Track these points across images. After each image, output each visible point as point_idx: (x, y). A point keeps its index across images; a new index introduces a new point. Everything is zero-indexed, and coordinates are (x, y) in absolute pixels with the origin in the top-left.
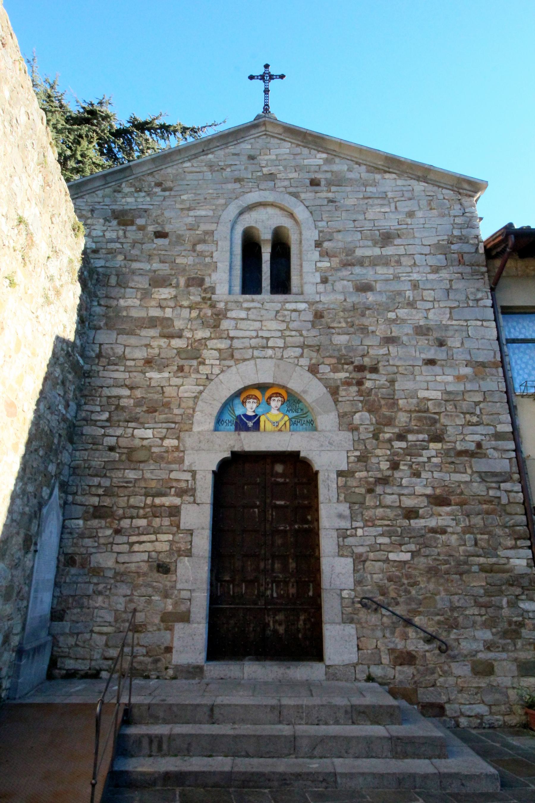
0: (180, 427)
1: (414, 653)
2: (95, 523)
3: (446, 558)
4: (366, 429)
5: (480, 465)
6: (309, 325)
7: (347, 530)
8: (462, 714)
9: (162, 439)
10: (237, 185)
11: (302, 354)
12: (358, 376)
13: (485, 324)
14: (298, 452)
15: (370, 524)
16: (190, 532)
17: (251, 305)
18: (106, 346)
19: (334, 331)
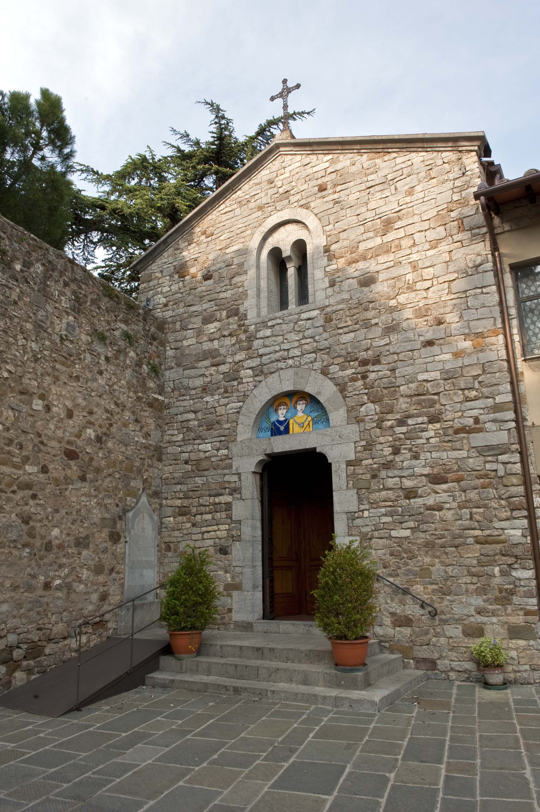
0: (228, 439)
1: (411, 617)
2: (180, 519)
3: (442, 532)
4: (371, 419)
5: (478, 440)
6: (321, 330)
7: (355, 512)
8: (452, 669)
9: (218, 450)
10: (260, 213)
11: (316, 358)
12: (361, 369)
13: (484, 290)
14: (315, 448)
15: (374, 506)
16: (239, 522)
17: (274, 322)
18: (177, 381)
19: (341, 331)
